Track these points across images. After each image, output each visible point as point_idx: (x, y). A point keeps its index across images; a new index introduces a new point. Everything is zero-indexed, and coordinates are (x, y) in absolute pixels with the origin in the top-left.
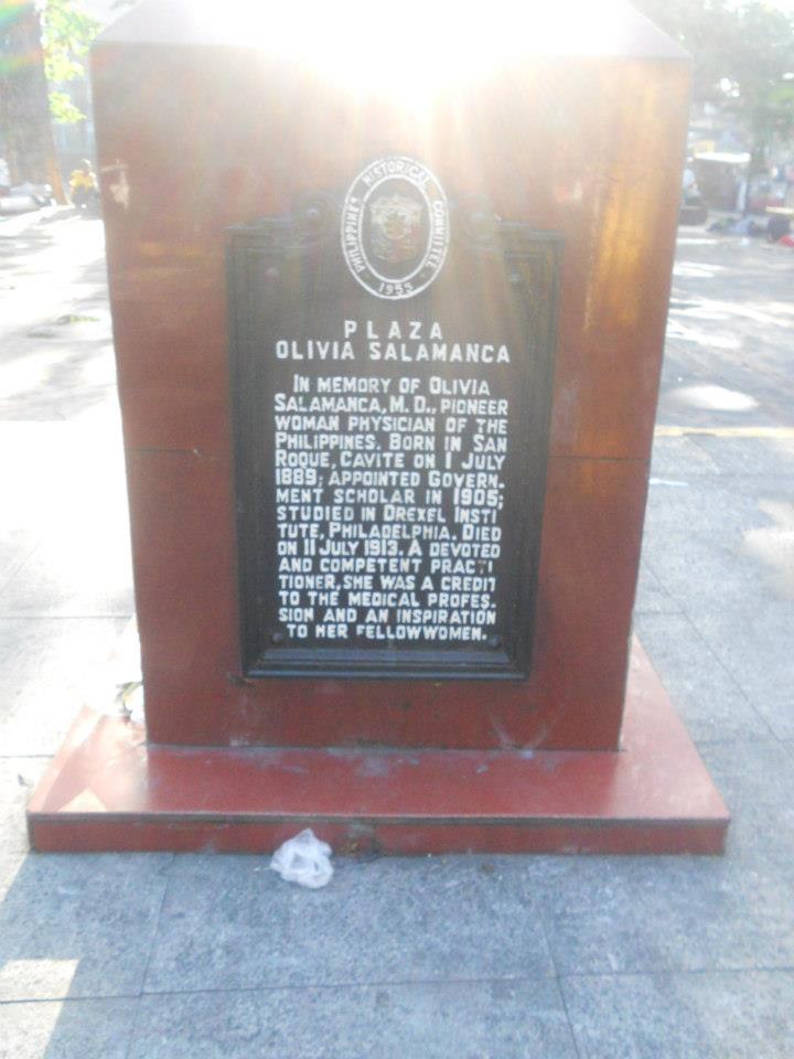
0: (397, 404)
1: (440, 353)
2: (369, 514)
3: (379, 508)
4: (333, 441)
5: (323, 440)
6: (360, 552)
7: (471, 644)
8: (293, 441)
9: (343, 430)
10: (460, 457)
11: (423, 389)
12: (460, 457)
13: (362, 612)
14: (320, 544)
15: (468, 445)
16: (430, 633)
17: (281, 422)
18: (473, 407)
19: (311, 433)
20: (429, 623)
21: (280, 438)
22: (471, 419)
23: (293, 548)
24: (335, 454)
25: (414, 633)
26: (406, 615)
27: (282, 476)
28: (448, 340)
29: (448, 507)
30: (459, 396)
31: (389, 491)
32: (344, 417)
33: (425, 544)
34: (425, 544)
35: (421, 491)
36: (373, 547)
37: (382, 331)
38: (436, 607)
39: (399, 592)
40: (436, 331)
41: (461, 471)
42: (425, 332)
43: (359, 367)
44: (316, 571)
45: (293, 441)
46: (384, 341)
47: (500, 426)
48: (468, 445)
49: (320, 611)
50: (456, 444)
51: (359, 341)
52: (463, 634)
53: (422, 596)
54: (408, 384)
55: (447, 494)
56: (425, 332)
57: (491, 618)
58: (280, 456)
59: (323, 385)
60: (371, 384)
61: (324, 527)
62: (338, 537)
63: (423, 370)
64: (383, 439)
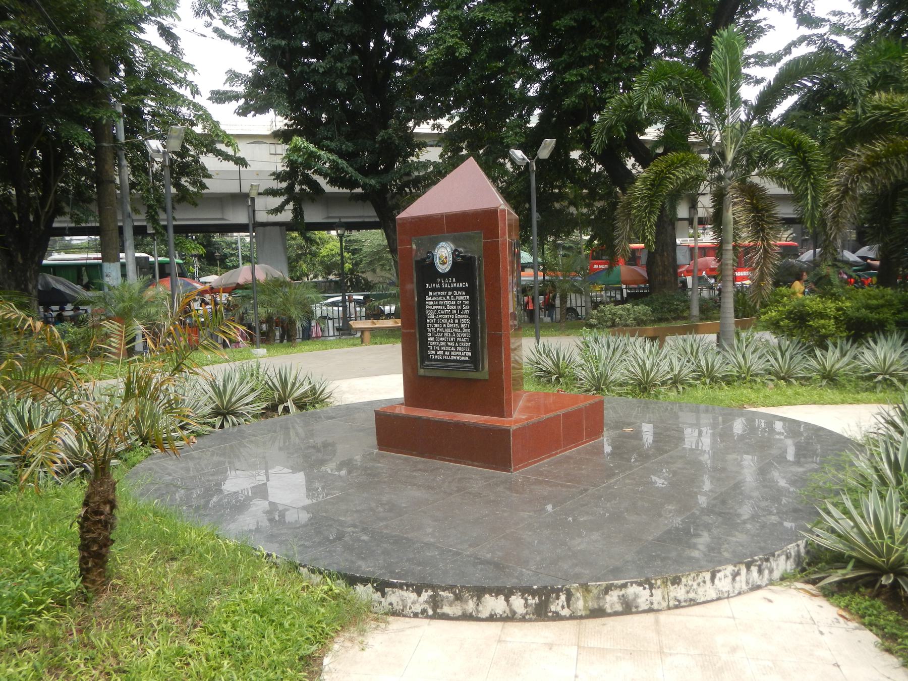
0: (448, 297)
1: (455, 285)
2: (445, 325)
3: (446, 324)
4: (437, 307)
5: (435, 307)
6: (443, 337)
7: (463, 361)
8: (429, 307)
9: (439, 305)
10: (461, 310)
11: (453, 294)
12: (461, 310)
13: (444, 351)
14: (436, 334)
15: (462, 307)
16: (458, 358)
17: (427, 303)
18: (462, 298)
19: (433, 306)
20: (458, 355)
21: (427, 307)
22: (462, 300)
23: (430, 334)
24: (437, 310)
25: (455, 358)
26: (453, 353)
27: (428, 316)
28: (457, 282)
29: (459, 324)
30: (459, 295)
31: (448, 319)
32: (438, 301)
33: (456, 333)
34: (456, 333)
35: (454, 319)
36: (446, 334)
37: (444, 280)
38: (459, 351)
39: (451, 346)
40: (454, 280)
41: (461, 314)
42: (452, 280)
43: (441, 289)
44: (435, 341)
45: (429, 307)
46: (445, 283)
47: (467, 302)
48: (462, 307)
49: (436, 351)
50: (459, 307)
51: (440, 283)
52: (464, 358)
53: (456, 347)
54: (450, 293)
55: (459, 320)
56: (452, 280)
57: (470, 354)
58: (427, 311)
59: (435, 294)
60: (443, 293)
61: (436, 330)
62: (439, 332)
63: (453, 289)
64: (446, 306)
